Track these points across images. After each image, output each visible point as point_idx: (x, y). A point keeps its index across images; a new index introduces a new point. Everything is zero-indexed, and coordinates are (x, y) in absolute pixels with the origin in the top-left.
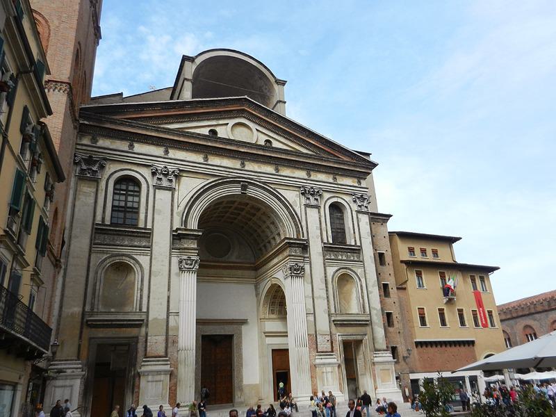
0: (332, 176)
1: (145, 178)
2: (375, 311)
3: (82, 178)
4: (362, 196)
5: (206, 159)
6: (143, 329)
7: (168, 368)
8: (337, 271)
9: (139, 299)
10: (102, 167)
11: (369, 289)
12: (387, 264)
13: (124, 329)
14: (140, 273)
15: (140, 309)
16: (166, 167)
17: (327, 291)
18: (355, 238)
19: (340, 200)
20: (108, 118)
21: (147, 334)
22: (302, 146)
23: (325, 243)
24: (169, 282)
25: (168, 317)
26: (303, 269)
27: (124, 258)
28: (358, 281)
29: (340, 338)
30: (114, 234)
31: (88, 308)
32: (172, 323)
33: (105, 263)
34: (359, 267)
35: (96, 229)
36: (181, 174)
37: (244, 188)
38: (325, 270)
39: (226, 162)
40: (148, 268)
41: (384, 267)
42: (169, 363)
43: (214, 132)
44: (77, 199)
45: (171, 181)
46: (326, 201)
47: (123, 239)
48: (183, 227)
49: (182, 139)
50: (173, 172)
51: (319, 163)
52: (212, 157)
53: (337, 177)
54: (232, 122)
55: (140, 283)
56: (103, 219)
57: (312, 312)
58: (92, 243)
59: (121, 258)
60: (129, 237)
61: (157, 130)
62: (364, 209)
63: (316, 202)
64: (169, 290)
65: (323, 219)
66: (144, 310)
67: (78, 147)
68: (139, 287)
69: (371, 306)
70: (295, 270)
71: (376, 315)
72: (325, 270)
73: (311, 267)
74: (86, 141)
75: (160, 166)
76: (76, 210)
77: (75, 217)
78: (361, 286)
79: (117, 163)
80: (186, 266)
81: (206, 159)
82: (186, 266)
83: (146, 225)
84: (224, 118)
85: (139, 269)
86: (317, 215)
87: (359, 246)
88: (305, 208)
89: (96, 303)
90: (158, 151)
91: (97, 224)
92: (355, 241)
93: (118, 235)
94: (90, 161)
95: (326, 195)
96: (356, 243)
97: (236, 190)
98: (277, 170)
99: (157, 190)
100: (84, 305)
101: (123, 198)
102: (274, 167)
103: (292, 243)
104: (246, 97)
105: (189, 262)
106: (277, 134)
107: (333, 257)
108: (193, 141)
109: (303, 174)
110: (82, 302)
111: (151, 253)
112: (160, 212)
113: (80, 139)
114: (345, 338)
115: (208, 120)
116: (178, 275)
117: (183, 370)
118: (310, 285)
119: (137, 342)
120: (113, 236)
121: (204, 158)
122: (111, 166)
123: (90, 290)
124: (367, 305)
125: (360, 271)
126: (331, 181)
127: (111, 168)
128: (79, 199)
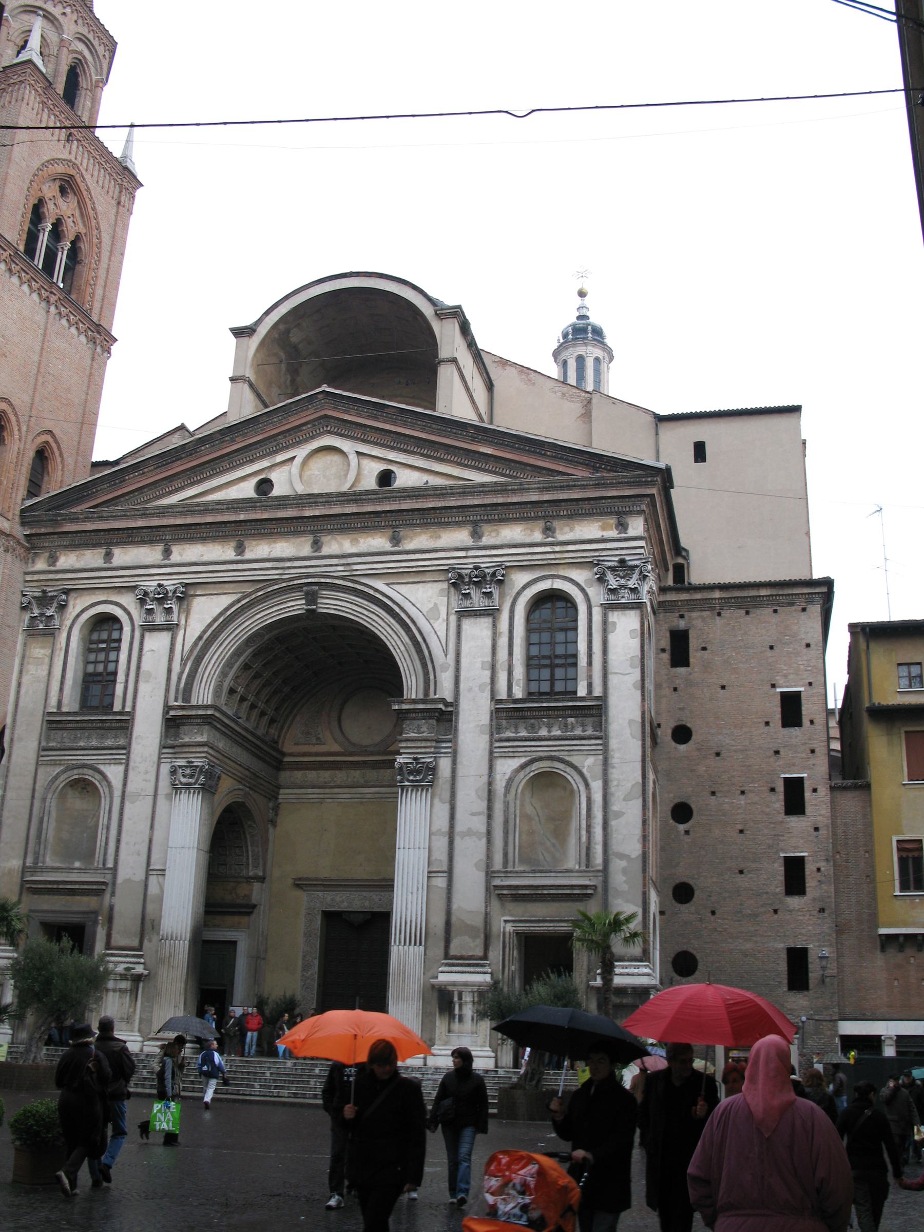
0: (541, 524)
1: (129, 614)
2: (623, 863)
3: (32, 632)
4: (622, 562)
5: (240, 549)
6: (107, 896)
7: (139, 969)
8: (523, 767)
9: (103, 844)
10: (62, 607)
11: (615, 807)
12: (806, 721)
13: (78, 897)
14: (108, 799)
15: (104, 864)
16: (160, 585)
17: (490, 817)
18: (590, 677)
19: (559, 584)
20: (67, 515)
21: (111, 908)
22: (466, 466)
23: (500, 701)
24: (154, 812)
25: (147, 878)
26: (432, 770)
27: (85, 771)
28: (582, 788)
29: (509, 928)
31: (29, 861)
32: (153, 889)
33: (57, 782)
34: (589, 753)
36: (192, 593)
37: (311, 598)
38: (491, 768)
39: (282, 548)
41: (795, 731)
42: (142, 961)
43: (265, 485)
44: (24, 673)
45: (169, 611)
46: (519, 594)
47: (89, 737)
48: (179, 703)
49: (189, 520)
50: (175, 592)
51: (500, 500)
52: (254, 543)
53: (556, 524)
54: (301, 452)
55: (106, 815)
57: (445, 868)
58: (43, 749)
59: (80, 771)
60: (113, 732)
61: (144, 515)
62: (626, 597)
63: (486, 602)
64: (152, 827)
65: (503, 641)
66: (110, 864)
67: (28, 578)
68: (106, 822)
69: (617, 845)
70: (411, 773)
71: (625, 871)
72: (491, 768)
74: (41, 565)
75: (150, 585)
76: (23, 691)
77: (21, 704)
78: (589, 799)
79: (86, 592)
80: (183, 780)
81: (240, 549)
82: (183, 780)
83: (124, 707)
84: (287, 448)
85: (107, 790)
87: (598, 698)
88: (459, 620)
89: (42, 852)
91: (50, 714)
92: (590, 685)
94: (44, 600)
95: (520, 578)
96: (590, 690)
97: (295, 606)
98: (395, 540)
99: (147, 635)
101: (102, 657)
102: (390, 532)
103: (408, 711)
104: (325, 388)
105: (188, 771)
106: (405, 451)
107: (523, 733)
108: (209, 519)
109: (460, 536)
110: (22, 853)
111: (128, 759)
113: (33, 562)
114: (522, 927)
115: (252, 461)
116: (169, 797)
117: (165, 975)
118: (447, 807)
119: (96, 922)
120: (73, 732)
122: (78, 601)
123: (33, 832)
124: (598, 849)
125: (589, 763)
126: (538, 536)
127: (77, 605)
128: (28, 671)
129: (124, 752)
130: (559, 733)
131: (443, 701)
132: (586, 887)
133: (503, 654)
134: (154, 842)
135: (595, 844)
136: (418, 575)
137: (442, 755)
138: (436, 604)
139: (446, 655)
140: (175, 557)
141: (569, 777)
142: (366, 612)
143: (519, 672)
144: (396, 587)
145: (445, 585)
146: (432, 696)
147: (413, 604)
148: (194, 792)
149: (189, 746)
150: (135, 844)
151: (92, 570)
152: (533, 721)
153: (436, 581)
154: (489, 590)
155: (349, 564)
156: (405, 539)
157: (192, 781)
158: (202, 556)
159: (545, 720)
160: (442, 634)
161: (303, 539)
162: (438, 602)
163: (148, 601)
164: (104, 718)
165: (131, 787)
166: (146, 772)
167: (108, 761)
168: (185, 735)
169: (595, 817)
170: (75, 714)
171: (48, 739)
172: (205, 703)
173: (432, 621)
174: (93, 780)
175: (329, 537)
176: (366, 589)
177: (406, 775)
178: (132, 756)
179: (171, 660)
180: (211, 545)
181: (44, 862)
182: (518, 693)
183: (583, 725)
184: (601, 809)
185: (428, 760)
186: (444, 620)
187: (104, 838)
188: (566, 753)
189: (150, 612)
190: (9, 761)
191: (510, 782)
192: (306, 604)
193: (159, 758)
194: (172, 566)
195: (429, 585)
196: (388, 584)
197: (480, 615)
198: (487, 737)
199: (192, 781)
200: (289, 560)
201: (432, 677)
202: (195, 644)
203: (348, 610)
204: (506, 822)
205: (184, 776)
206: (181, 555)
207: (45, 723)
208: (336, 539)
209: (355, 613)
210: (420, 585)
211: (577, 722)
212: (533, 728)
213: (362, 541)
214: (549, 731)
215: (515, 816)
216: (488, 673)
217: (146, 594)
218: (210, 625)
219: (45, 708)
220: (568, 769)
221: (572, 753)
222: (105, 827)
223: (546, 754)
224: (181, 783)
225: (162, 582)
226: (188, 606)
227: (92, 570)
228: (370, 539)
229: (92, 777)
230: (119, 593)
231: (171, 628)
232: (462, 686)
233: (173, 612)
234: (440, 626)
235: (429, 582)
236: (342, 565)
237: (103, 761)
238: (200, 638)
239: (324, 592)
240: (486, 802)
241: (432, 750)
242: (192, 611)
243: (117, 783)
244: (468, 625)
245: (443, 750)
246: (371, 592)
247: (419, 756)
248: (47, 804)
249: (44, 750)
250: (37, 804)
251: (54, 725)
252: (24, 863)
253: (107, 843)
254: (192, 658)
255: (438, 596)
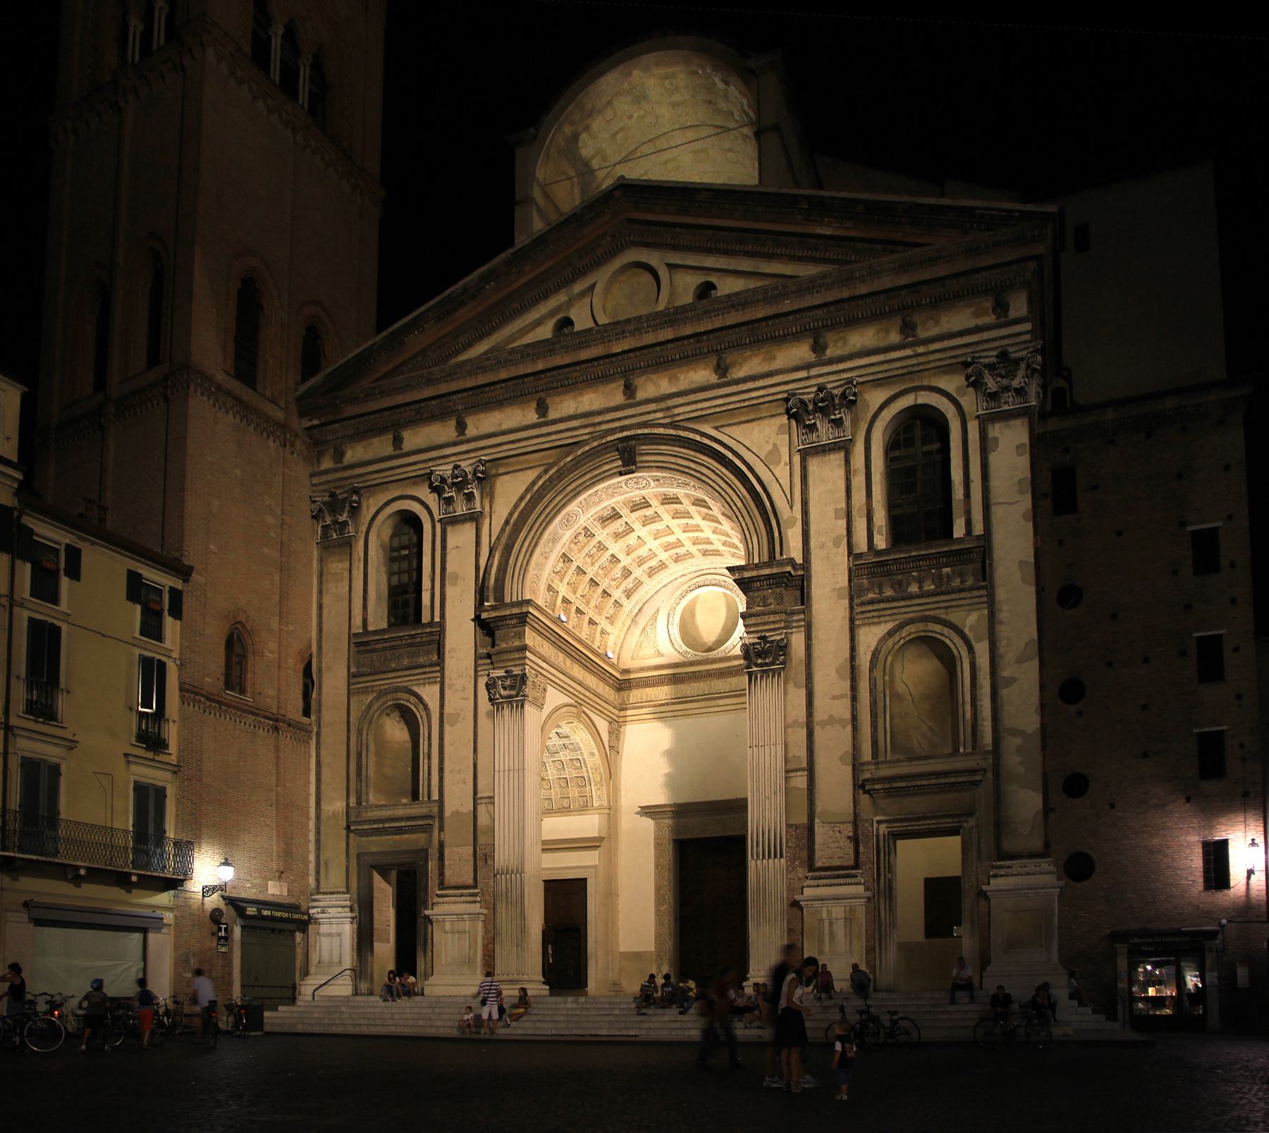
5: (542, 409)
8: (890, 634)
9: (426, 775)
17: (854, 699)
23: (860, 555)
27: (400, 695)
28: (964, 652)
30: (385, 649)
33: (372, 711)
35: (358, 644)
36: (494, 472)
39: (590, 400)
40: (437, 710)
50: (475, 473)
52: (557, 399)
55: (426, 743)
56: (365, 621)
59: (394, 696)
68: (426, 751)
69: (1008, 722)
70: (759, 655)
73: (809, 638)
81: (542, 409)
85: (424, 714)
86: (842, 472)
90: (443, 431)
91: (356, 635)
93: (393, 648)
98: (722, 370)
100: (348, 798)
110: (345, 794)
111: (443, 676)
112: (456, 577)
116: (491, 715)
121: (538, 411)
129: (438, 668)
130: (933, 587)
131: (791, 561)
132: (972, 771)
133: (859, 498)
134: (479, 767)
135: (983, 720)
136: (752, 412)
137: (794, 630)
138: (775, 445)
139: (791, 507)
140: (471, 431)
141: (948, 641)
142: (693, 466)
143: (880, 517)
144: (727, 430)
145: (784, 419)
146: (778, 556)
147: (748, 449)
148: (517, 706)
149: (507, 652)
150: (459, 772)
151: (382, 460)
152: (900, 577)
153: (773, 416)
154: (838, 416)
155: (669, 408)
156: (732, 368)
157: (513, 693)
158: (501, 424)
159: (915, 574)
160: (785, 482)
161: (613, 385)
162: (778, 442)
163: (447, 488)
164: (413, 633)
165: (447, 709)
166: (464, 689)
167: (422, 681)
168: (501, 641)
169: (981, 687)
170: (382, 631)
171: (358, 665)
172: (520, 599)
173: (771, 467)
174: (408, 704)
175: (643, 378)
176: (691, 436)
177: (754, 659)
178: (447, 673)
179: (477, 555)
180: (509, 410)
181: (367, 801)
182: (881, 542)
183: (961, 575)
184: (988, 677)
185: (778, 638)
186: (786, 464)
187: (426, 769)
188: (943, 611)
189: (449, 501)
190: (320, 694)
191: (875, 654)
192: (623, 466)
193: (476, 671)
194: (468, 441)
195: (766, 421)
196: (716, 428)
197: (830, 450)
198: (846, 602)
199: (513, 693)
200: (600, 413)
201: (776, 534)
202: (503, 530)
203: (672, 466)
204: (874, 704)
205: (505, 688)
206: (478, 428)
207: (352, 645)
208: (651, 380)
209: (681, 469)
210: (754, 424)
211: (953, 572)
212: (900, 586)
213: (682, 377)
214: (920, 588)
215: (885, 696)
216: (843, 523)
217: (443, 480)
218: (516, 506)
219: (350, 629)
220: (946, 631)
221: (949, 610)
222: (426, 756)
223: (918, 614)
224: (502, 697)
225: (458, 463)
226: (491, 489)
227: (382, 460)
228: (691, 374)
229: (407, 701)
230: (415, 483)
231: (475, 518)
232: (813, 543)
233: (474, 498)
234: (782, 472)
235: (765, 417)
236: (661, 410)
237: (416, 682)
238: (507, 522)
239: (643, 447)
240: (849, 681)
241: (782, 625)
242: (495, 494)
243: (434, 705)
244: (814, 465)
245: (795, 624)
246: (698, 438)
247: (767, 635)
248: (364, 737)
249: (355, 676)
250: (353, 739)
251: (362, 648)
252: (348, 805)
253: (429, 774)
254: (500, 548)
255: (777, 434)
